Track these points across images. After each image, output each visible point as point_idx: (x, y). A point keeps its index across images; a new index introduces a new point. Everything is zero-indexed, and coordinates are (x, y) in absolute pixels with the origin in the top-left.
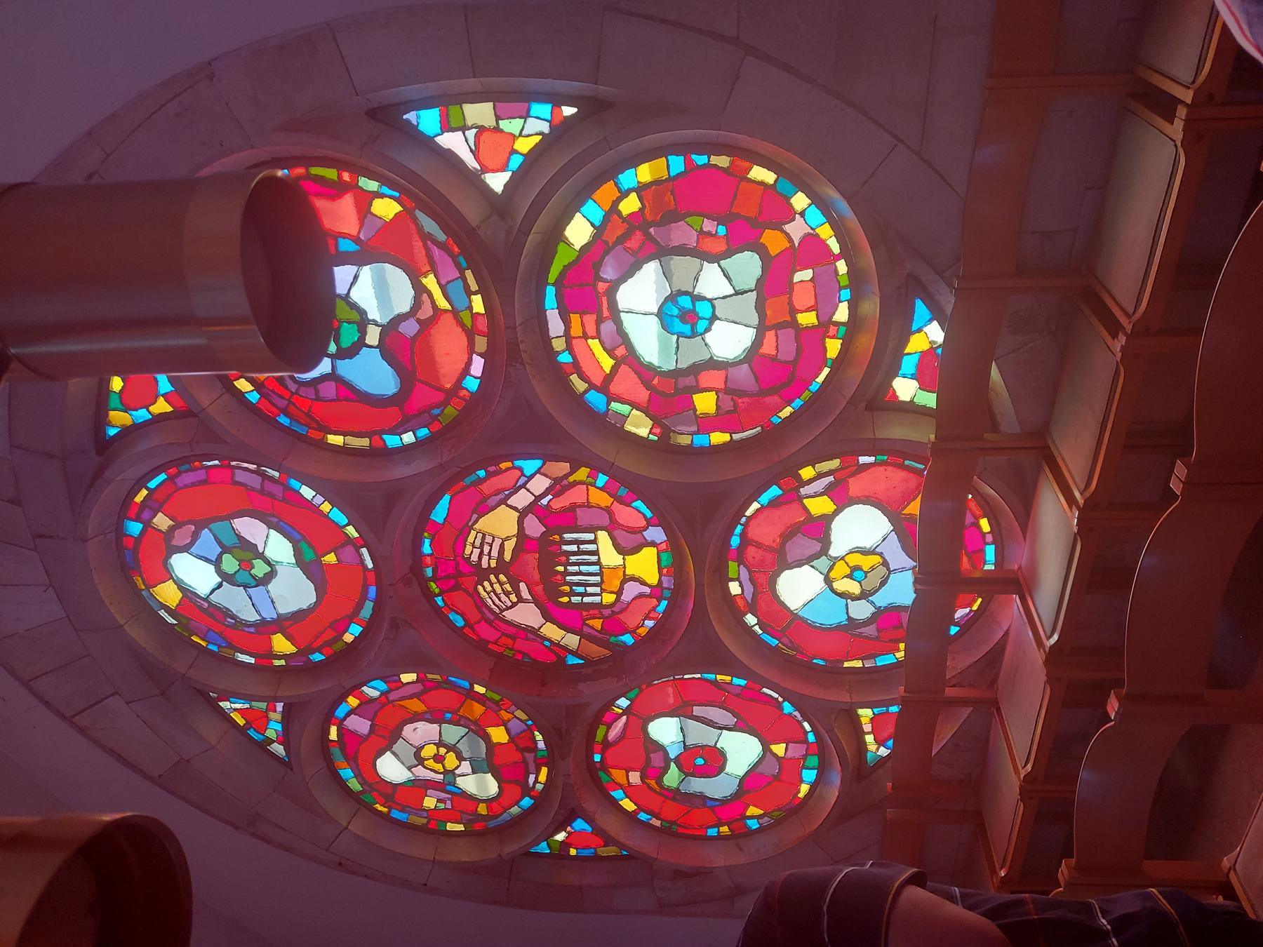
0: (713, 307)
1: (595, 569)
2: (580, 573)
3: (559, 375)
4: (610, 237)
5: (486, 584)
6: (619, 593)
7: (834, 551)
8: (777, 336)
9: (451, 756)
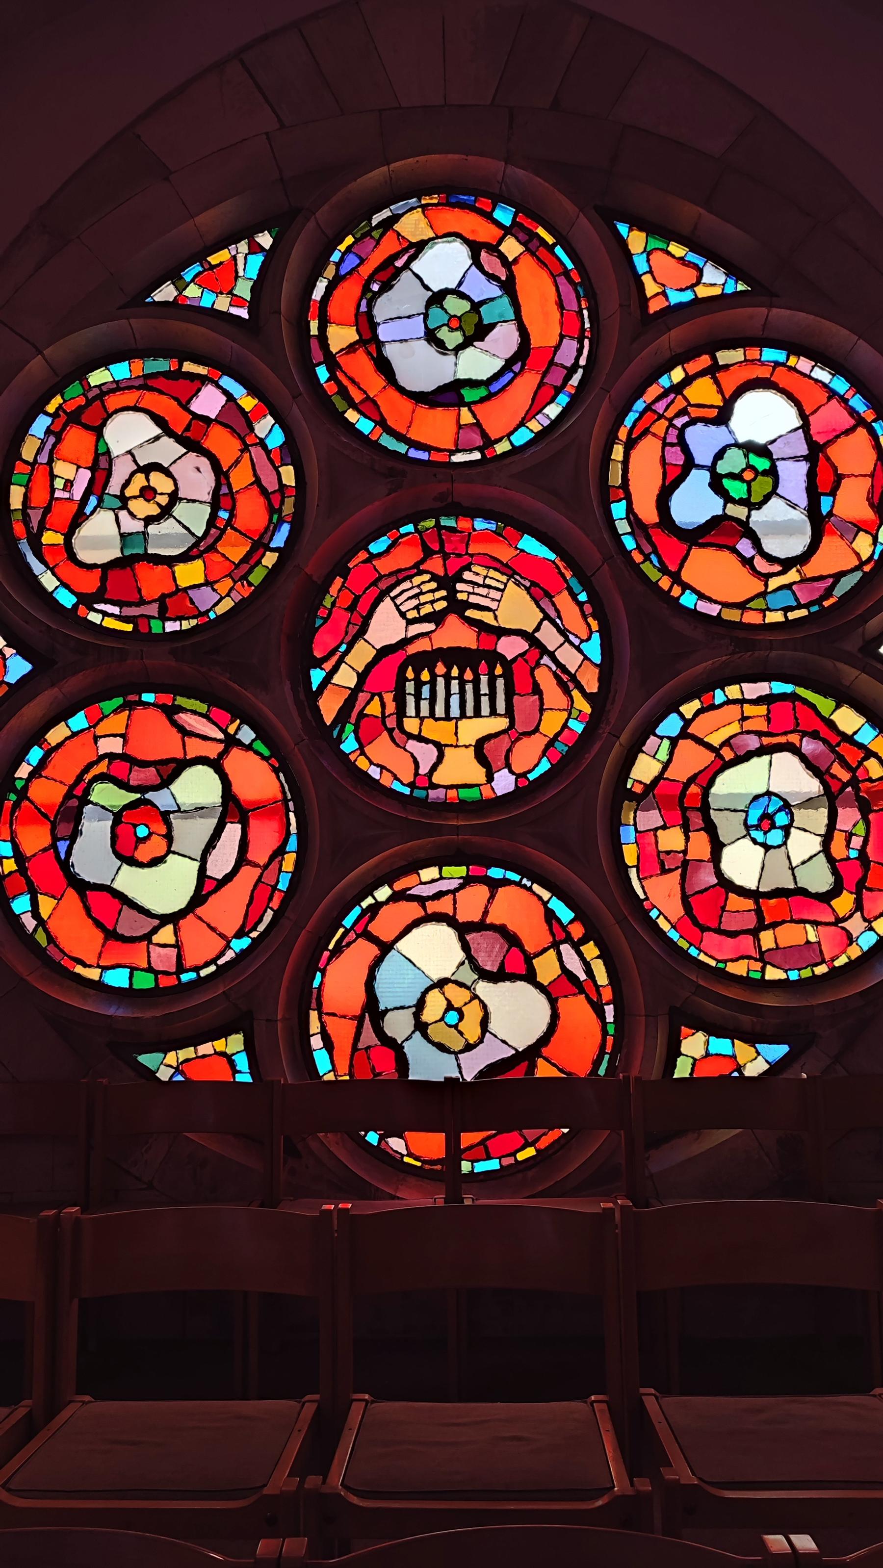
0: (779, 846)
1: (455, 711)
2: (448, 695)
3: (700, 689)
4: (843, 748)
5: (433, 585)
6: (420, 738)
7: (483, 989)
8: (749, 911)
9: (154, 510)
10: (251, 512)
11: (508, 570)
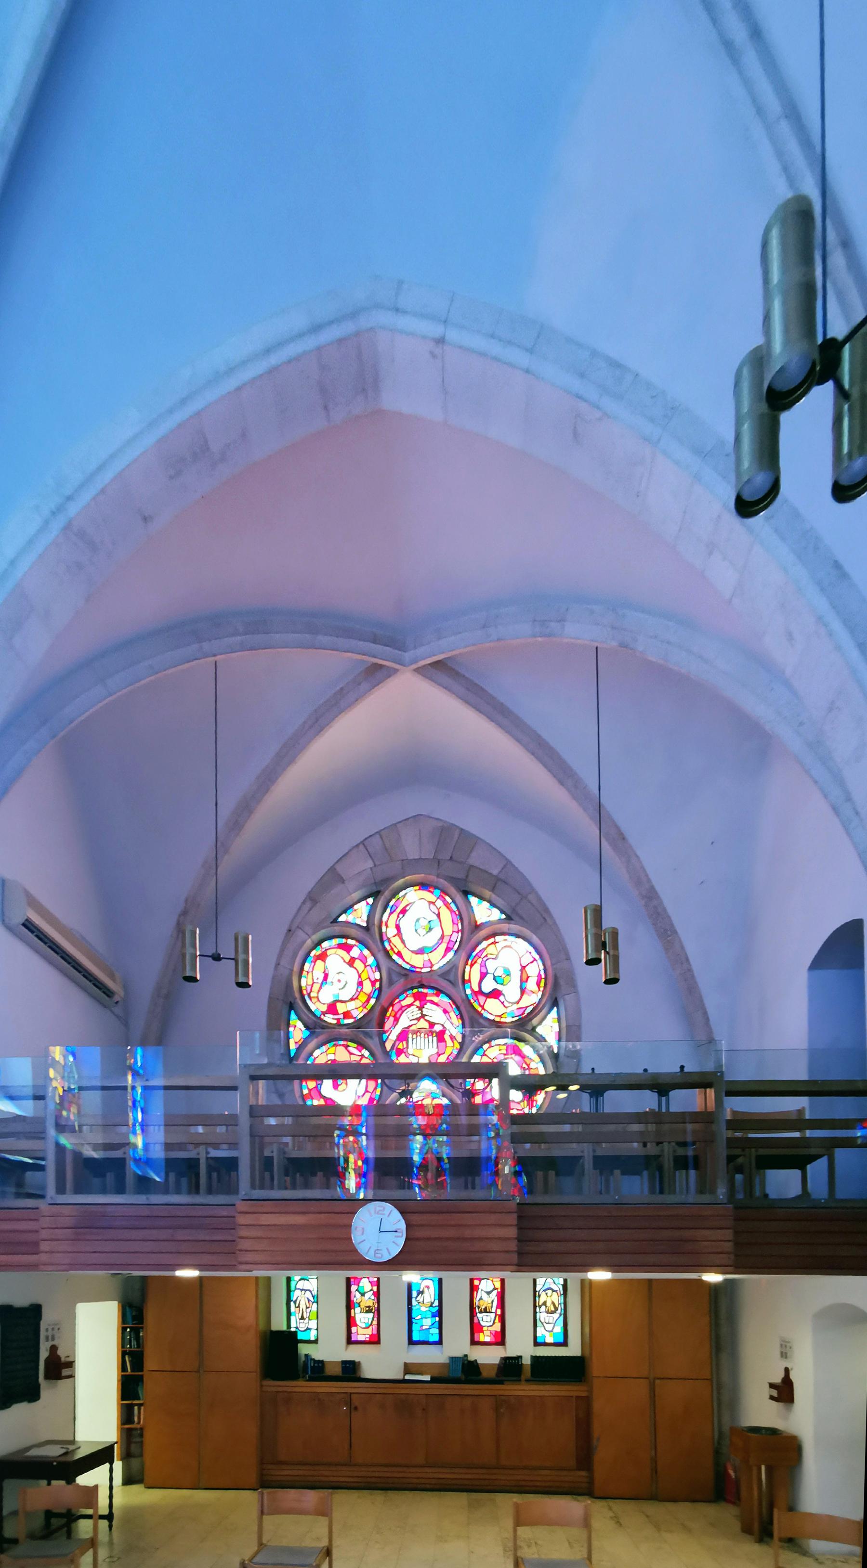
1: (422, 1047)
4: (526, 1060)
10: (367, 987)
11: (436, 1004)
